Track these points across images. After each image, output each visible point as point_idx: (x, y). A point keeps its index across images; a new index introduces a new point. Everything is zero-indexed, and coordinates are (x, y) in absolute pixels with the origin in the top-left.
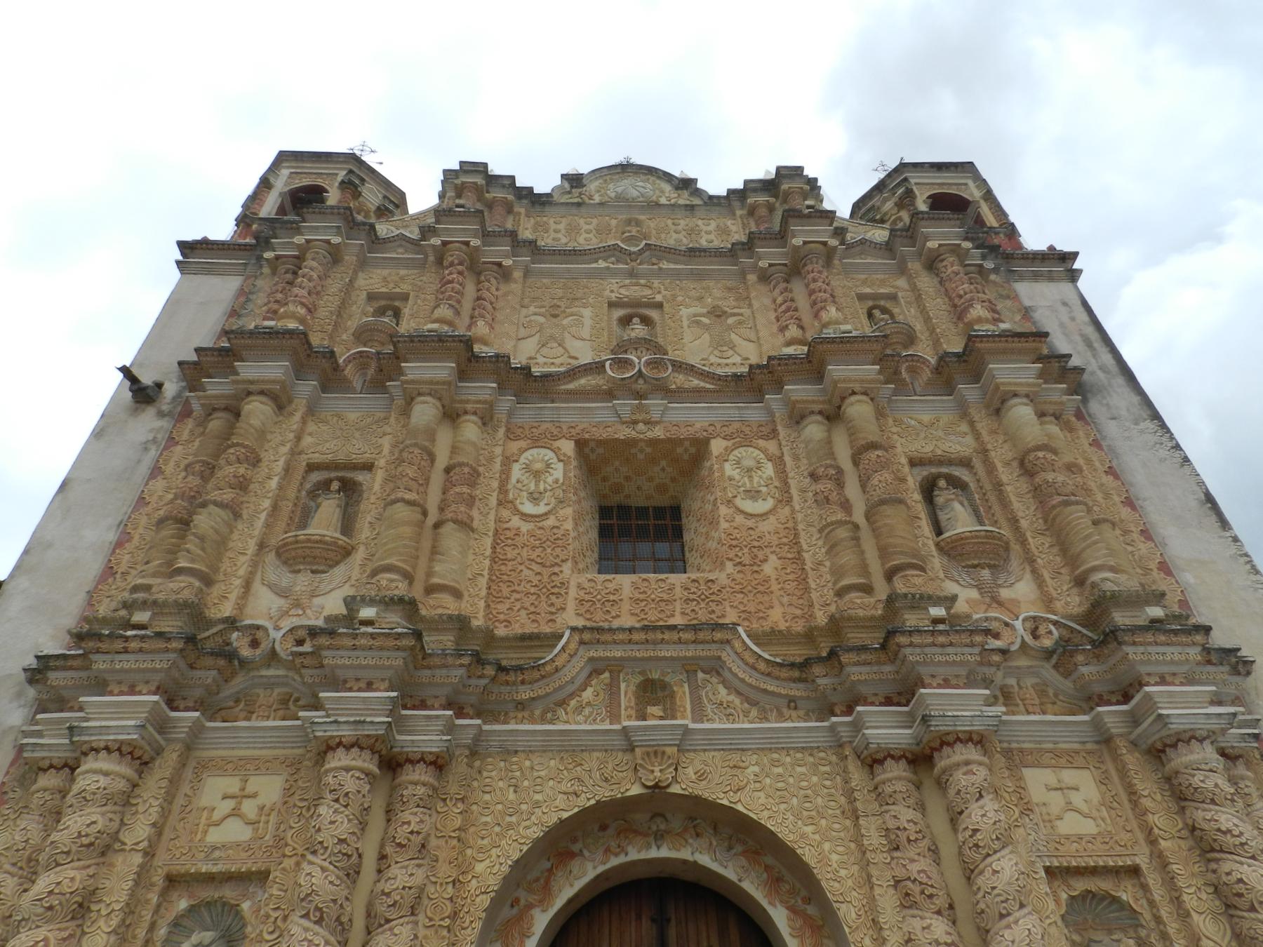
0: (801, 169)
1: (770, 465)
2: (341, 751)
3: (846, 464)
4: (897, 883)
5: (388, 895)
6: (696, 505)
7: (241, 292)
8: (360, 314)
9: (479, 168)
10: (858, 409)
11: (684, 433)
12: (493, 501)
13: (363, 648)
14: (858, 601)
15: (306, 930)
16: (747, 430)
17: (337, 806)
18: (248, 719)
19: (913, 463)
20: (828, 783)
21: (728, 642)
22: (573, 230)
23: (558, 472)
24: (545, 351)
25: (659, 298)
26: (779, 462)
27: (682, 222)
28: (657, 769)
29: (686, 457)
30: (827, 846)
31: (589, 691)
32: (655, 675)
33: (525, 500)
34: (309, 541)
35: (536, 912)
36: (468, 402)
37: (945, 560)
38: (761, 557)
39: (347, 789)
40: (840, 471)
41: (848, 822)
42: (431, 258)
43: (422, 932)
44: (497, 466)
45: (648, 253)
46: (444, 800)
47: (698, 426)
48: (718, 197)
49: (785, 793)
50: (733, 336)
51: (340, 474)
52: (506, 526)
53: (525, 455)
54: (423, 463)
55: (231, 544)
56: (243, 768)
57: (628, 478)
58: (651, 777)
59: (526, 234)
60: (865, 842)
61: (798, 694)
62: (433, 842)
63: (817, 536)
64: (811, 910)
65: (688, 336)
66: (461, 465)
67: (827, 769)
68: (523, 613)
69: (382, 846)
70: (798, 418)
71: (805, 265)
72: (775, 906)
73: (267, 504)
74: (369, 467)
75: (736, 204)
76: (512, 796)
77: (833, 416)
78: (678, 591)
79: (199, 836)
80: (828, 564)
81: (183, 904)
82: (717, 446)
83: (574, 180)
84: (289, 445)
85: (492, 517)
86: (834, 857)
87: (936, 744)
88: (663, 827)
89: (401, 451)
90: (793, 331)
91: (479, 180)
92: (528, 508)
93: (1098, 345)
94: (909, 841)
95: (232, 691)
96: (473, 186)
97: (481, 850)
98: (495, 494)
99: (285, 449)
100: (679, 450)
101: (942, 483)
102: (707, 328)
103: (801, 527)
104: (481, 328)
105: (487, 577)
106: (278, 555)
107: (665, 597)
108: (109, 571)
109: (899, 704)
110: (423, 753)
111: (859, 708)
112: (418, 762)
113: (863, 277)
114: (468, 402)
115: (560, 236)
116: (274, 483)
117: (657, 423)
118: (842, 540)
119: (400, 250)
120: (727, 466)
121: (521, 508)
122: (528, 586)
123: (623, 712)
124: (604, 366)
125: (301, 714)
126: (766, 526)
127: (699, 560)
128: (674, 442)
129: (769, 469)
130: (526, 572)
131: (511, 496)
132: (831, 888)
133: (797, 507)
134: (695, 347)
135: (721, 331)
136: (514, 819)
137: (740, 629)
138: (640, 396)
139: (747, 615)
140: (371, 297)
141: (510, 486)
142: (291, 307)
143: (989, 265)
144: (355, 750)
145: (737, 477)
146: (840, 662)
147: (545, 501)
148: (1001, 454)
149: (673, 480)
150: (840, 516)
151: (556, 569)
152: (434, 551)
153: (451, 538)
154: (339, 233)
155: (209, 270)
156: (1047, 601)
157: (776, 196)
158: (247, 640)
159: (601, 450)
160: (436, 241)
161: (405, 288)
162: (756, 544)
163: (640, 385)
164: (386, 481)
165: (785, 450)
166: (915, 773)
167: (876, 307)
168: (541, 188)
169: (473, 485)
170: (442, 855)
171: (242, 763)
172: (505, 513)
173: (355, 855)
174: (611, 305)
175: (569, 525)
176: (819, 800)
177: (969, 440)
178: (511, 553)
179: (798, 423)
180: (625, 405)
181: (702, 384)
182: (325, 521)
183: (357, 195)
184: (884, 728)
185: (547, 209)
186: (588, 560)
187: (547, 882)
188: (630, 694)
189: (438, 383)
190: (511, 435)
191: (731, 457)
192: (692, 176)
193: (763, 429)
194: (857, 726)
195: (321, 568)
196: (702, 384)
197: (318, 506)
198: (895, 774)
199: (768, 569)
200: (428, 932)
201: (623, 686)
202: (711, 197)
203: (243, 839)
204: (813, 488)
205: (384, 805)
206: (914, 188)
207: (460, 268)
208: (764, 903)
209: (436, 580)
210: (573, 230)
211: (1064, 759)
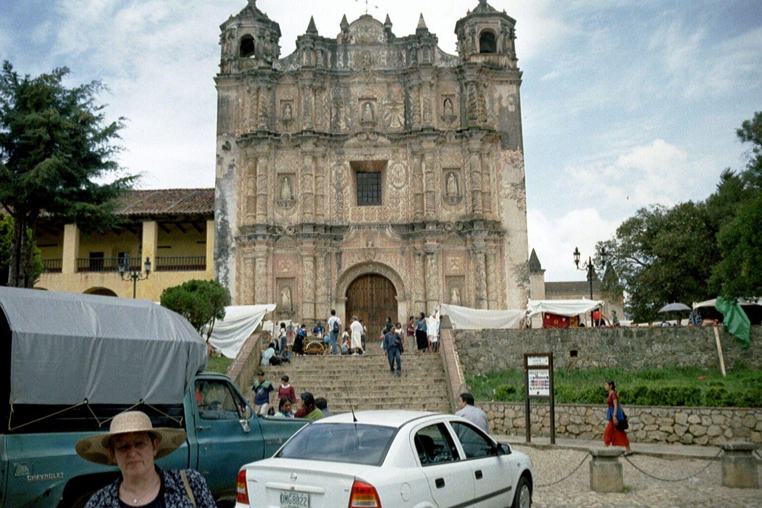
1: (404, 171)
25: (375, 96)
26: (406, 168)
82: (390, 163)
120: (393, 171)
140: (281, 101)
209: (318, 213)
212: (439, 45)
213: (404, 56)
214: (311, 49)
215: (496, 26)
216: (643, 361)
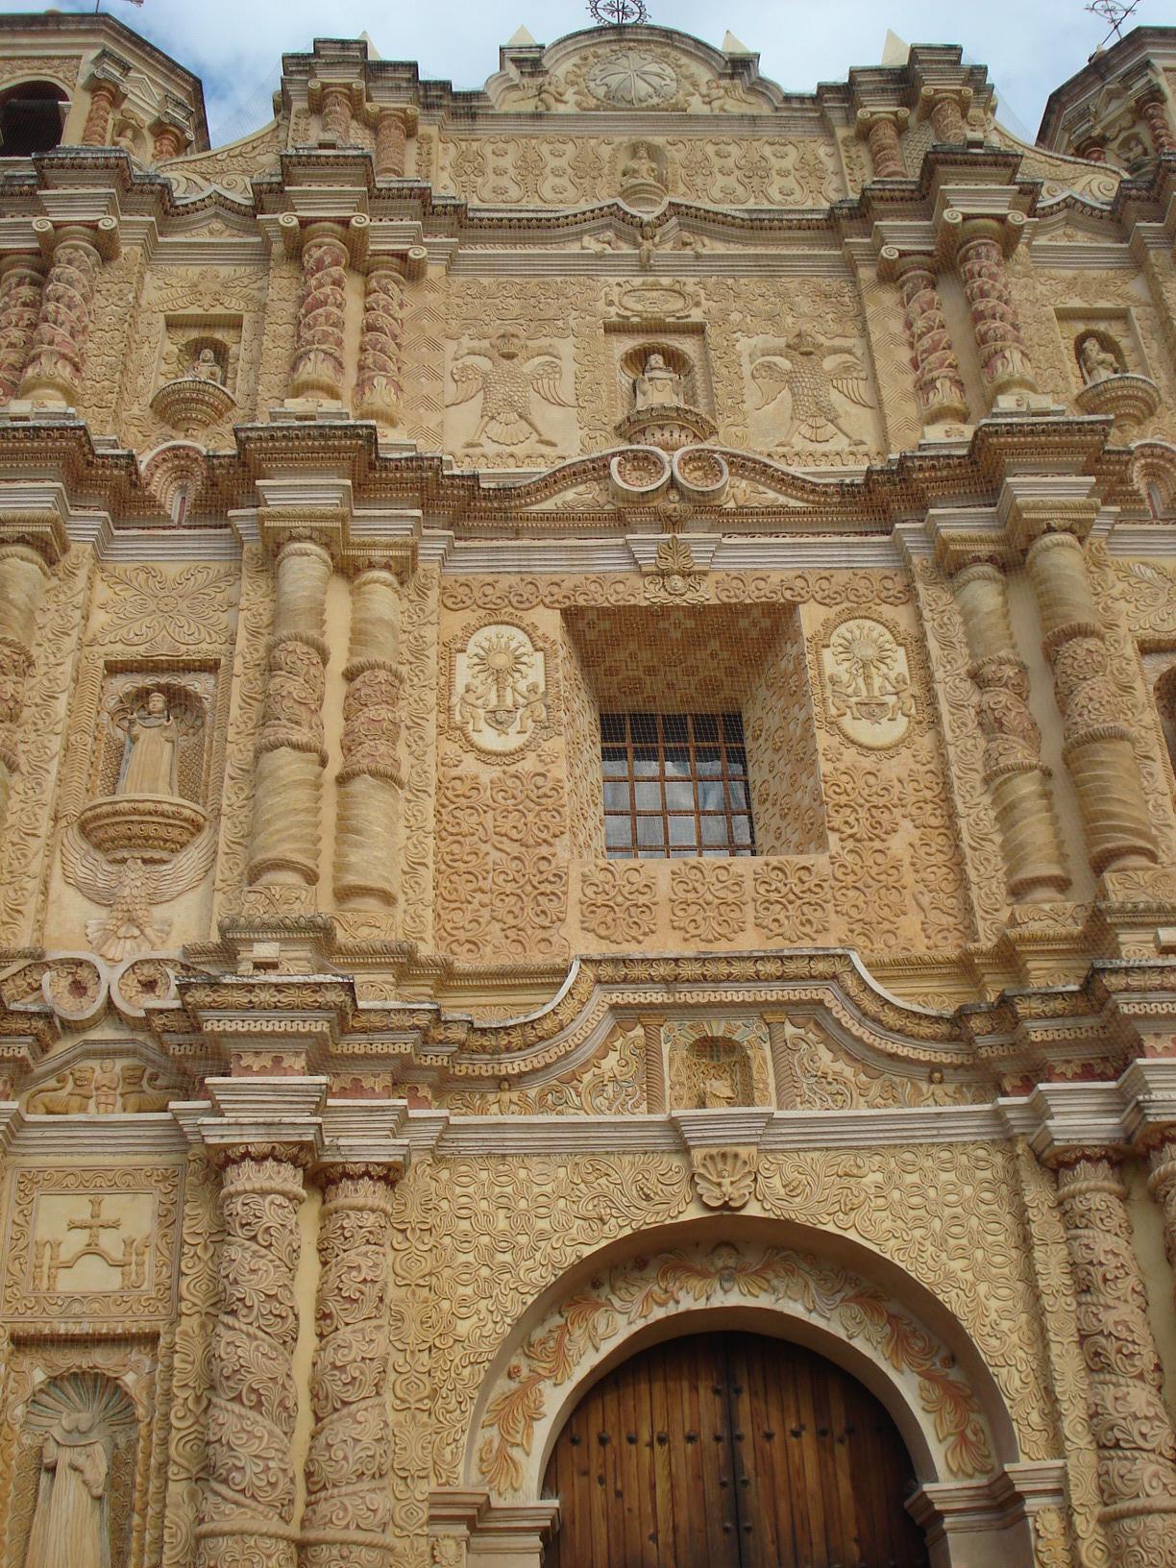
0: (955, 50)
2: (248, 1165)
3: (1033, 658)
4: (1083, 1338)
5: (342, 1369)
6: (772, 722)
8: (159, 364)
9: (350, 53)
10: (1062, 558)
12: (431, 730)
13: (265, 1007)
14: (1047, 907)
15: (241, 1416)
16: (861, 585)
17: (255, 1247)
18: (83, 1109)
19: (1146, 649)
20: (987, 1196)
21: (835, 977)
23: (534, 672)
24: (495, 429)
25: (696, 316)
27: (733, 149)
28: (726, 1181)
29: (754, 634)
30: (982, 1288)
31: (613, 1056)
32: (717, 1029)
33: (482, 725)
34: (135, 811)
35: (546, 1386)
36: (374, 546)
38: (887, 826)
39: (266, 1222)
40: (1023, 669)
41: (1014, 1253)
42: (278, 248)
43: (392, 1417)
44: (432, 665)
45: (674, 220)
46: (403, 1231)
47: (775, 579)
48: (801, 99)
49: (923, 1212)
50: (835, 396)
51: (163, 680)
52: (455, 772)
53: (480, 637)
54: (313, 670)
55: (11, 819)
56: (91, 1183)
57: (651, 671)
58: (717, 1192)
59: (444, 187)
60: (1041, 1283)
61: (946, 1059)
62: (393, 1293)
63: (980, 788)
64: (954, 1375)
66: (372, 667)
67: (987, 1174)
68: (498, 926)
69: (321, 1300)
70: (950, 567)
71: (966, 259)
72: (901, 1372)
73: (56, 745)
74: (210, 667)
75: (836, 116)
76: (502, 1224)
77: (1013, 560)
78: (749, 884)
79: (45, 1284)
80: (998, 839)
81: (39, 1376)
82: (810, 618)
83: (526, 61)
84: (75, 633)
85: (431, 759)
86: (993, 1304)
87: (1155, 1140)
88: (731, 1263)
89: (270, 648)
90: (945, 395)
91: (352, 78)
92: (489, 739)
94: (1105, 1280)
95: (54, 1064)
96: (332, 78)
97: (463, 1301)
98: (432, 717)
99: (69, 643)
100: (743, 623)
102: (790, 380)
103: (954, 770)
104: (381, 395)
105: (432, 867)
106: (85, 829)
107: (731, 898)
109: (1103, 1077)
110: (367, 1164)
111: (1041, 1086)
112: (361, 1177)
113: (1070, 273)
114: (374, 546)
115: (505, 182)
116: (61, 706)
117: (705, 573)
118: (1023, 798)
119: (217, 225)
120: (826, 653)
121: (475, 737)
122: (500, 879)
123: (668, 1092)
124: (606, 466)
125: (173, 1105)
126: (893, 769)
127: (776, 822)
128: (731, 611)
129: (900, 663)
130: (495, 855)
131: (458, 718)
132: (987, 1347)
133: (949, 736)
134: (762, 422)
135: (813, 392)
136: (507, 1257)
137: (855, 957)
138: (671, 523)
140: (173, 324)
141: (455, 700)
142: (47, 367)
144: (270, 1163)
145: (845, 677)
146: (1015, 1014)
147: (517, 725)
149: (730, 672)
150: (1020, 753)
151: (544, 850)
152: (346, 827)
153: (373, 804)
154: (111, 210)
157: (908, 102)
158: (65, 982)
159: (606, 625)
160: (289, 220)
161: (232, 306)
162: (881, 802)
163: (672, 504)
164: (248, 699)
165: (928, 626)
166: (1121, 1181)
167: (1094, 336)
169: (392, 701)
170: (412, 1311)
171: (87, 1176)
172: (451, 749)
173: (291, 1317)
174: (610, 329)
175: (560, 771)
176: (974, 1222)
178: (468, 821)
179: (951, 575)
180: (647, 542)
181: (782, 500)
182: (151, 773)
183: (116, 98)
184: (1078, 1114)
185: (480, 123)
186: (590, 824)
187: (560, 1343)
188: (677, 1062)
189: (323, 517)
190: (452, 602)
191: (834, 639)
192: (752, 50)
193: (889, 584)
194: (1039, 1112)
195: (157, 855)
196: (782, 500)
197: (134, 740)
198: (1092, 1184)
199: (899, 845)
200: (401, 1416)
201: (666, 1049)
202: (788, 98)
203: (110, 1288)
204: (975, 699)
205: (315, 1241)
206: (1162, 81)
207: (337, 271)
208: (885, 1366)
209: (351, 879)
210: (530, 170)
212: (1000, 117)
213: (830, 164)
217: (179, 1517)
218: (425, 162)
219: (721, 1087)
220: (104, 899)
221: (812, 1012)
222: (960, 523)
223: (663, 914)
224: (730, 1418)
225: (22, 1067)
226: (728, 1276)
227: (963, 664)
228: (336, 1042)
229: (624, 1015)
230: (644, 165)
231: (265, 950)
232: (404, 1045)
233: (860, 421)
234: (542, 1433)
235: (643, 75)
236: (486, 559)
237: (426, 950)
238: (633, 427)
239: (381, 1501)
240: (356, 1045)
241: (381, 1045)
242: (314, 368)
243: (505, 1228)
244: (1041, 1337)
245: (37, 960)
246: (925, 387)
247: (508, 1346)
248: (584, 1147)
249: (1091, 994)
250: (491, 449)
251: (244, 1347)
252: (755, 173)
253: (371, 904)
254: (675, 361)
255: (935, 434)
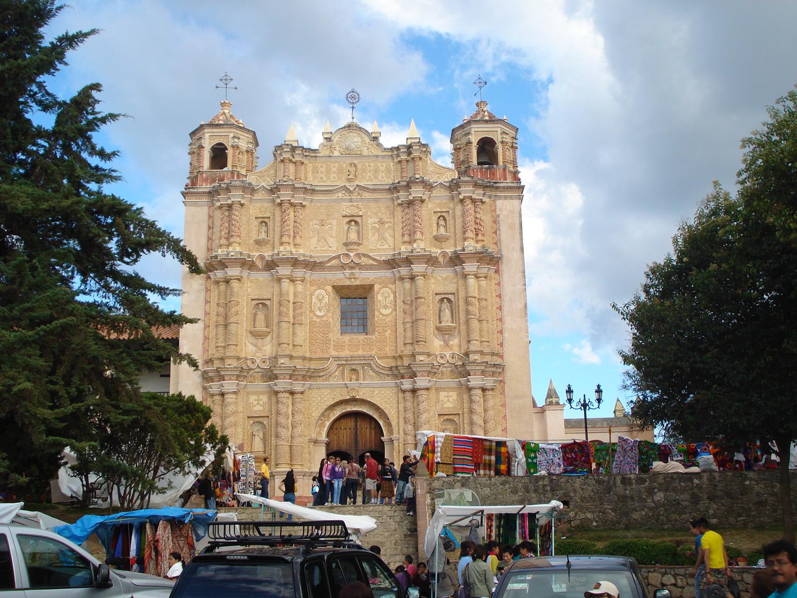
7: (210, 217)
10: (420, 281)
11: (366, 283)
22: (328, 171)
23: (327, 300)
37: (436, 332)
56: (256, 393)
59: (311, 180)
65: (370, 235)
70: (402, 279)
82: (376, 287)
90: (406, 238)
92: (318, 313)
93: (518, 236)
101: (445, 301)
102: (378, 230)
104: (298, 241)
108: (206, 338)
115: (323, 176)
126: (388, 319)
129: (392, 298)
138: (352, 268)
139: (380, 350)
143: (485, 199)
148: (462, 294)
155: (195, 204)
156: (460, 346)
161: (268, 215)
168: (315, 146)
175: (330, 320)
177: (455, 285)
178: (315, 330)
180: (347, 272)
183: (237, 147)
184: (407, 384)
190: (312, 284)
199: (387, 334)
210: (328, 171)
211: (452, 389)
214: (291, 161)
215: (495, 132)
216: (643, 513)
217: (273, 442)
218: (306, 173)
219: (354, 377)
220: (255, 345)
221: (369, 365)
222: (404, 271)
223: (347, 347)
224: (356, 426)
225: (245, 376)
226: (355, 406)
227: (402, 299)
228: (293, 375)
229: (339, 365)
230: (352, 169)
231: (282, 361)
232: (304, 373)
233: (390, 240)
234: (326, 429)
235: (355, 140)
236: (317, 275)
237: (307, 355)
238: (346, 244)
239: (301, 440)
240: (297, 373)
241: (300, 373)
242: (285, 239)
243: (320, 401)
244: (398, 417)
245: (246, 359)
246: (403, 235)
247: (320, 417)
248: (332, 387)
249: (409, 367)
250: (319, 248)
251: (281, 420)
252: (376, 171)
253: (299, 347)
254: (356, 222)
255: (403, 249)
